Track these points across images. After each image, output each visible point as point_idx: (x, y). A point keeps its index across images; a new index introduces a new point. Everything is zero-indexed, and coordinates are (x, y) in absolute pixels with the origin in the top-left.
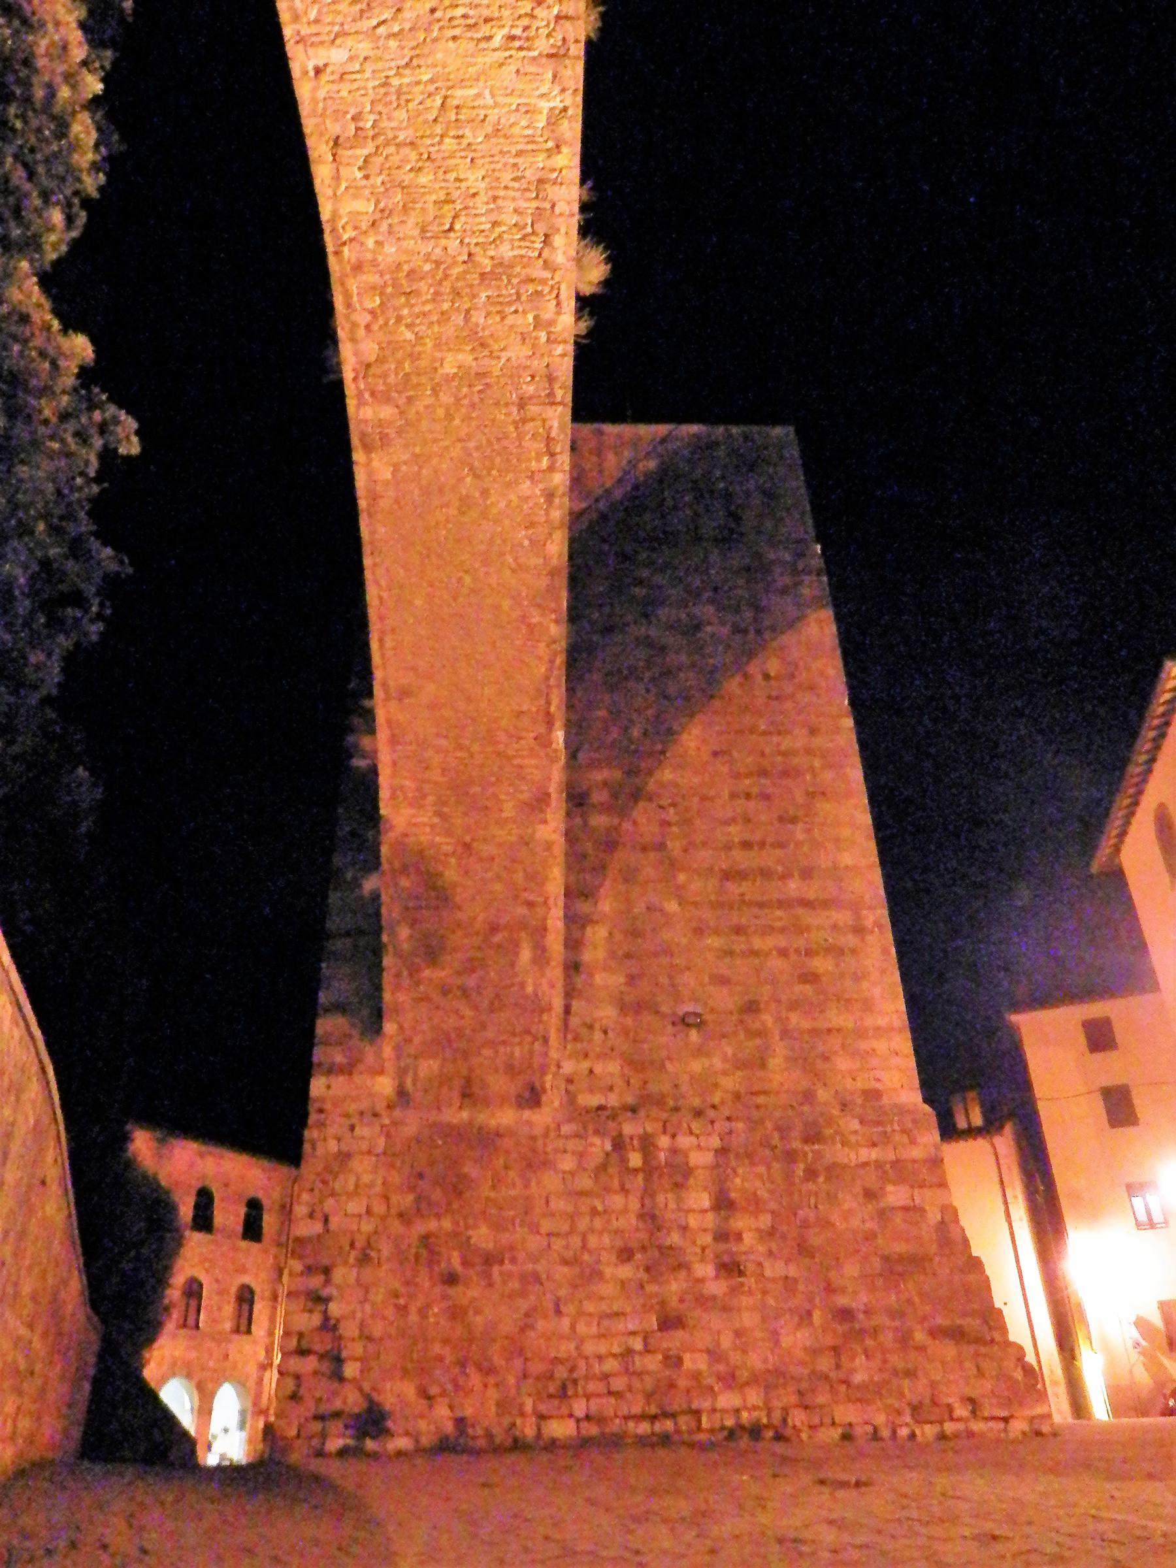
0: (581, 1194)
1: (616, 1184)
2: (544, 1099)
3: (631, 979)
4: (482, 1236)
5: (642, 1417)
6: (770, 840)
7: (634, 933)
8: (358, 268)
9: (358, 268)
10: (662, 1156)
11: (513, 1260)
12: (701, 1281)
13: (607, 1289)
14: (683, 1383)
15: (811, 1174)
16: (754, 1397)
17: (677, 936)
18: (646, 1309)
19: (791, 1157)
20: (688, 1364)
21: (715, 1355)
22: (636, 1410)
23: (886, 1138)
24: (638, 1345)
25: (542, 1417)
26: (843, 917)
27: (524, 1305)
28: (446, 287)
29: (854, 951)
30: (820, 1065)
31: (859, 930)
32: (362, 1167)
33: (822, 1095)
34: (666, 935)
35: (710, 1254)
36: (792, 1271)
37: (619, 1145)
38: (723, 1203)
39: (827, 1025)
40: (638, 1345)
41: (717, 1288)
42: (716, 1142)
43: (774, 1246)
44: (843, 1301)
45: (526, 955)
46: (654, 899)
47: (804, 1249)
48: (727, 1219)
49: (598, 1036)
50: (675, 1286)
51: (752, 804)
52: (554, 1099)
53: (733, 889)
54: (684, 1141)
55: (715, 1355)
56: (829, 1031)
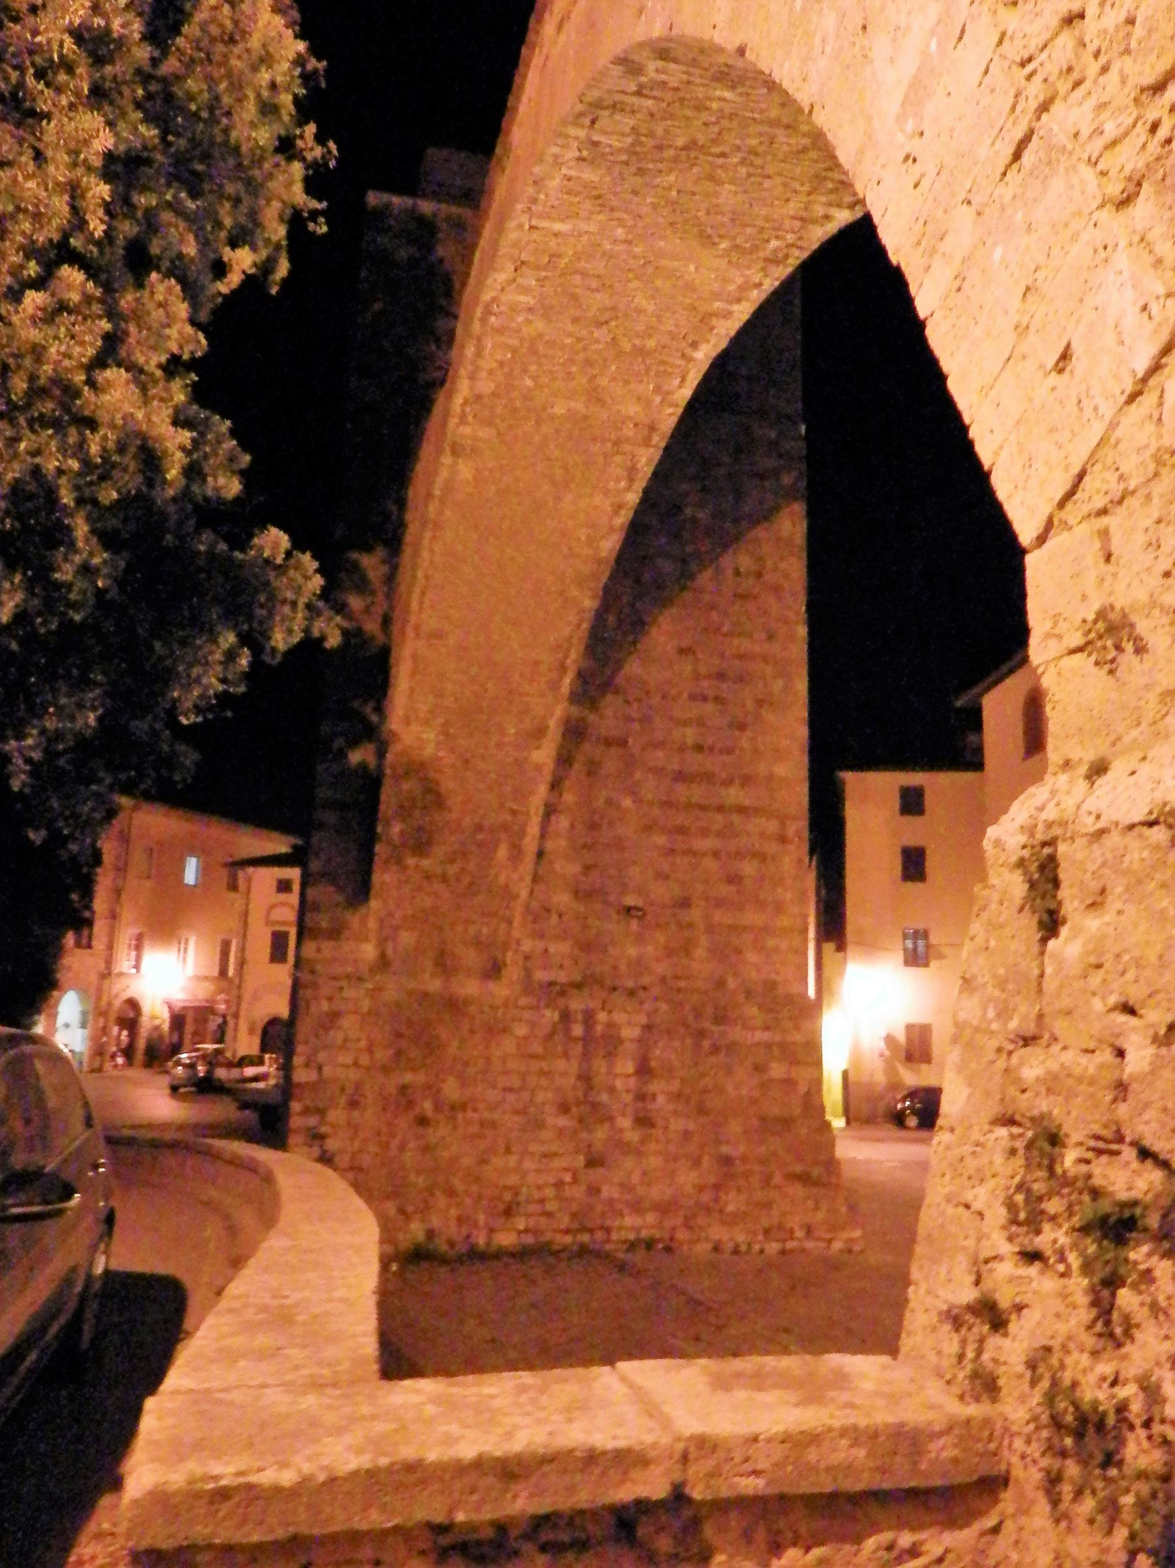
0: (534, 1056)
1: (560, 1049)
2: (504, 972)
3: (587, 869)
4: (451, 1090)
5: (567, 1231)
6: (719, 745)
7: (593, 826)
8: (499, 331)
9: (499, 331)
11: (475, 1110)
12: (621, 1130)
13: (545, 1135)
15: (715, 1050)
16: (651, 1218)
17: (627, 830)
18: (577, 1152)
19: (701, 1034)
21: (626, 1187)
22: (563, 1226)
24: (568, 1178)
25: (492, 1230)
26: (772, 826)
27: (482, 1145)
28: (581, 356)
29: (773, 858)
31: (783, 839)
32: (348, 1023)
33: (732, 983)
34: (621, 830)
35: (629, 1110)
36: (692, 1126)
37: (566, 1017)
38: (644, 1070)
40: (568, 1178)
42: (643, 1019)
44: (725, 1150)
45: (502, 853)
47: (702, 1110)
48: (645, 1083)
49: (554, 919)
50: (600, 1133)
52: (513, 972)
53: (682, 792)
54: (619, 1017)
55: (626, 1187)
56: (745, 928)
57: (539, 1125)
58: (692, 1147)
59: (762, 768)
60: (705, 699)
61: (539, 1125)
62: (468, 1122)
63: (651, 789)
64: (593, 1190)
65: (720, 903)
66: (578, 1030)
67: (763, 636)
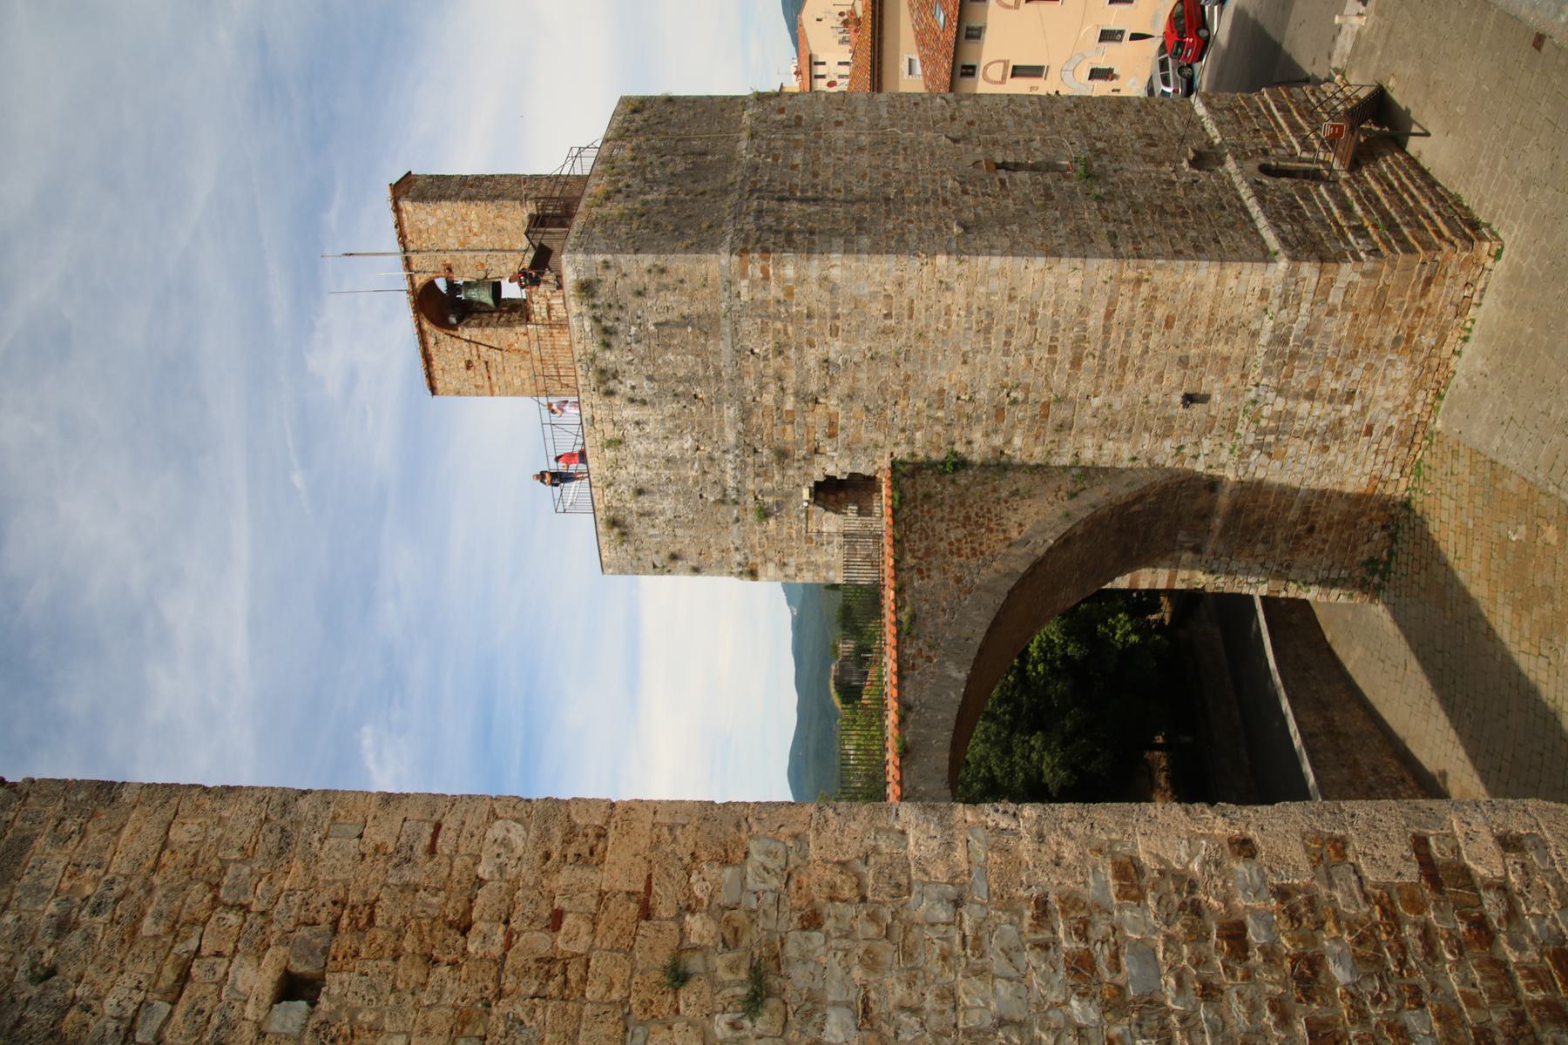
3: (1147, 429)
4: (1293, 515)
7: (1114, 425)
15: (1310, 344)
16: (1421, 396)
21: (1394, 412)
23: (1298, 296)
30: (1235, 323)
38: (1310, 397)
40: (1375, 447)
41: (1357, 405)
44: (1388, 342)
46: (1090, 412)
50: (1350, 426)
51: (1014, 342)
54: (1266, 411)
57: (1332, 463)
58: (1381, 365)
59: (1071, 298)
60: (1007, 344)
62: (1318, 504)
63: (1083, 385)
65: (1187, 332)
66: (1271, 438)
67: (948, 294)
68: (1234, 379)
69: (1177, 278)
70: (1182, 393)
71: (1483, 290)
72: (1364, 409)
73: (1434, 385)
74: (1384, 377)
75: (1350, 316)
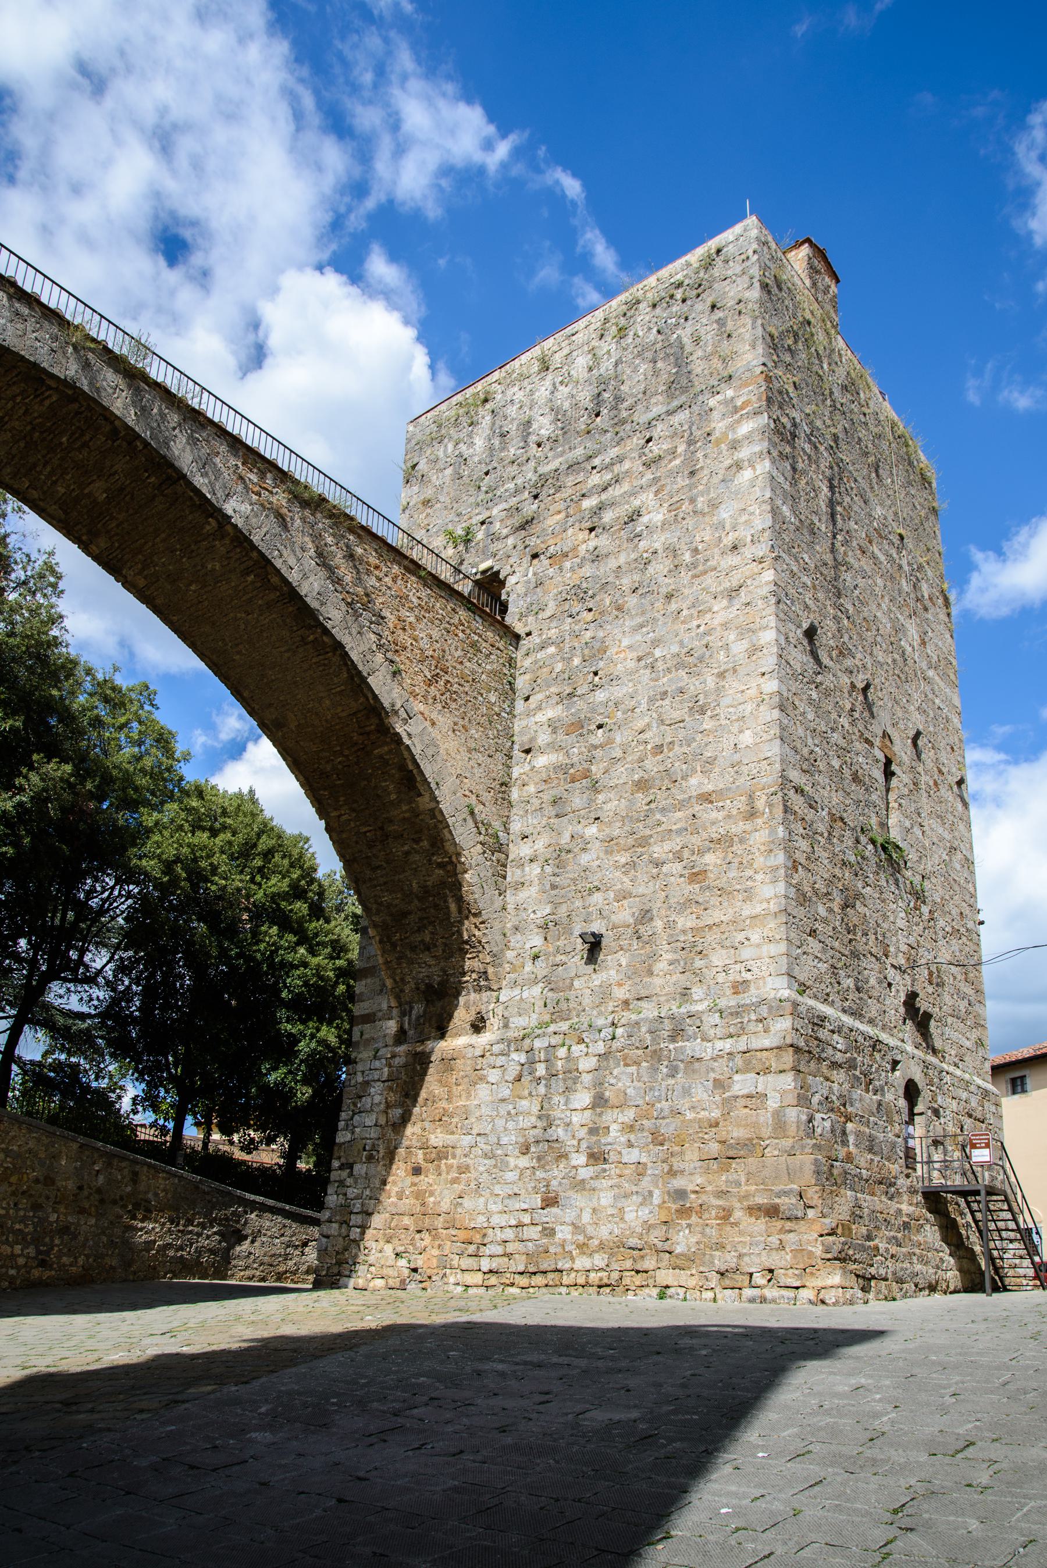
0: (503, 1100)
10: (560, 1063)
11: (454, 1157)
13: (510, 1176)
14: (552, 1250)
20: (559, 1235)
21: (576, 1228)
22: (521, 1268)
27: (458, 1188)
30: (699, 963)
33: (697, 992)
35: (584, 1145)
38: (600, 1102)
39: (710, 922)
43: (632, 1137)
44: (678, 1183)
48: (600, 1115)
50: (557, 1173)
55: (576, 1228)
56: (710, 927)
57: (503, 1167)
58: (646, 1183)
61: (503, 1167)
62: (449, 1167)
64: (549, 1232)
68: (620, 993)
69: (760, 861)
70: (603, 931)
71: (763, 1300)
72: (580, 1185)
73: (615, 1275)
74: (626, 1196)
75: (716, 1114)
